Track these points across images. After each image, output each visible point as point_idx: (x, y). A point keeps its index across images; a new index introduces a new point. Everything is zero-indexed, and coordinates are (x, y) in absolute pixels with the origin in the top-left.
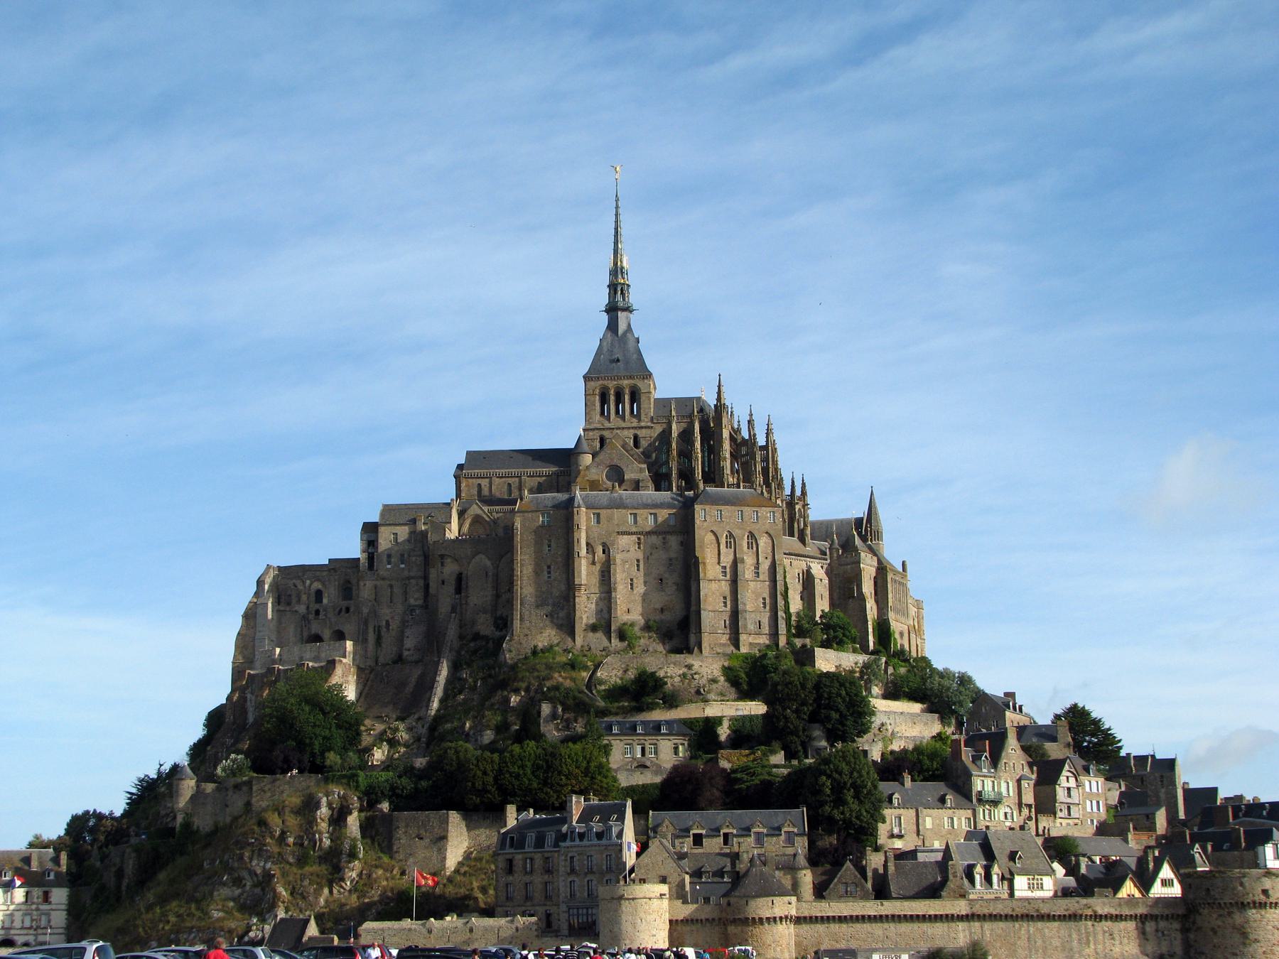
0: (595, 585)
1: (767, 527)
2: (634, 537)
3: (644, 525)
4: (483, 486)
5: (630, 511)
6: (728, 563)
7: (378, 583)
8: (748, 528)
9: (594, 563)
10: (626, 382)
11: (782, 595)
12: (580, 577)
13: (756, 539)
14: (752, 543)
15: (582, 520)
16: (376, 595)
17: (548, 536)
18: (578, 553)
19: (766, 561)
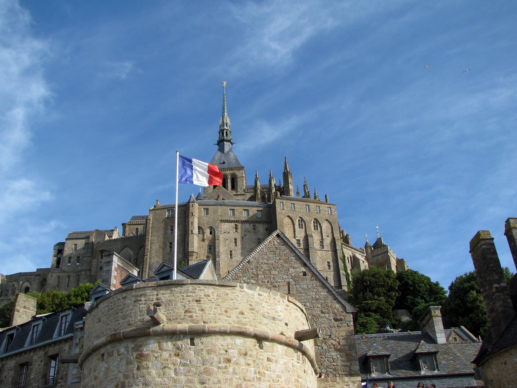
0: (204, 255)
1: (327, 217)
2: (233, 224)
3: (240, 217)
4: (139, 230)
5: (229, 208)
6: (301, 237)
7: (61, 275)
8: (314, 216)
9: (203, 240)
10: (228, 172)
11: (341, 259)
12: (193, 247)
13: (320, 224)
14: (317, 226)
15: (195, 211)
16: (58, 283)
17: (171, 224)
18: (192, 231)
19: (328, 238)
